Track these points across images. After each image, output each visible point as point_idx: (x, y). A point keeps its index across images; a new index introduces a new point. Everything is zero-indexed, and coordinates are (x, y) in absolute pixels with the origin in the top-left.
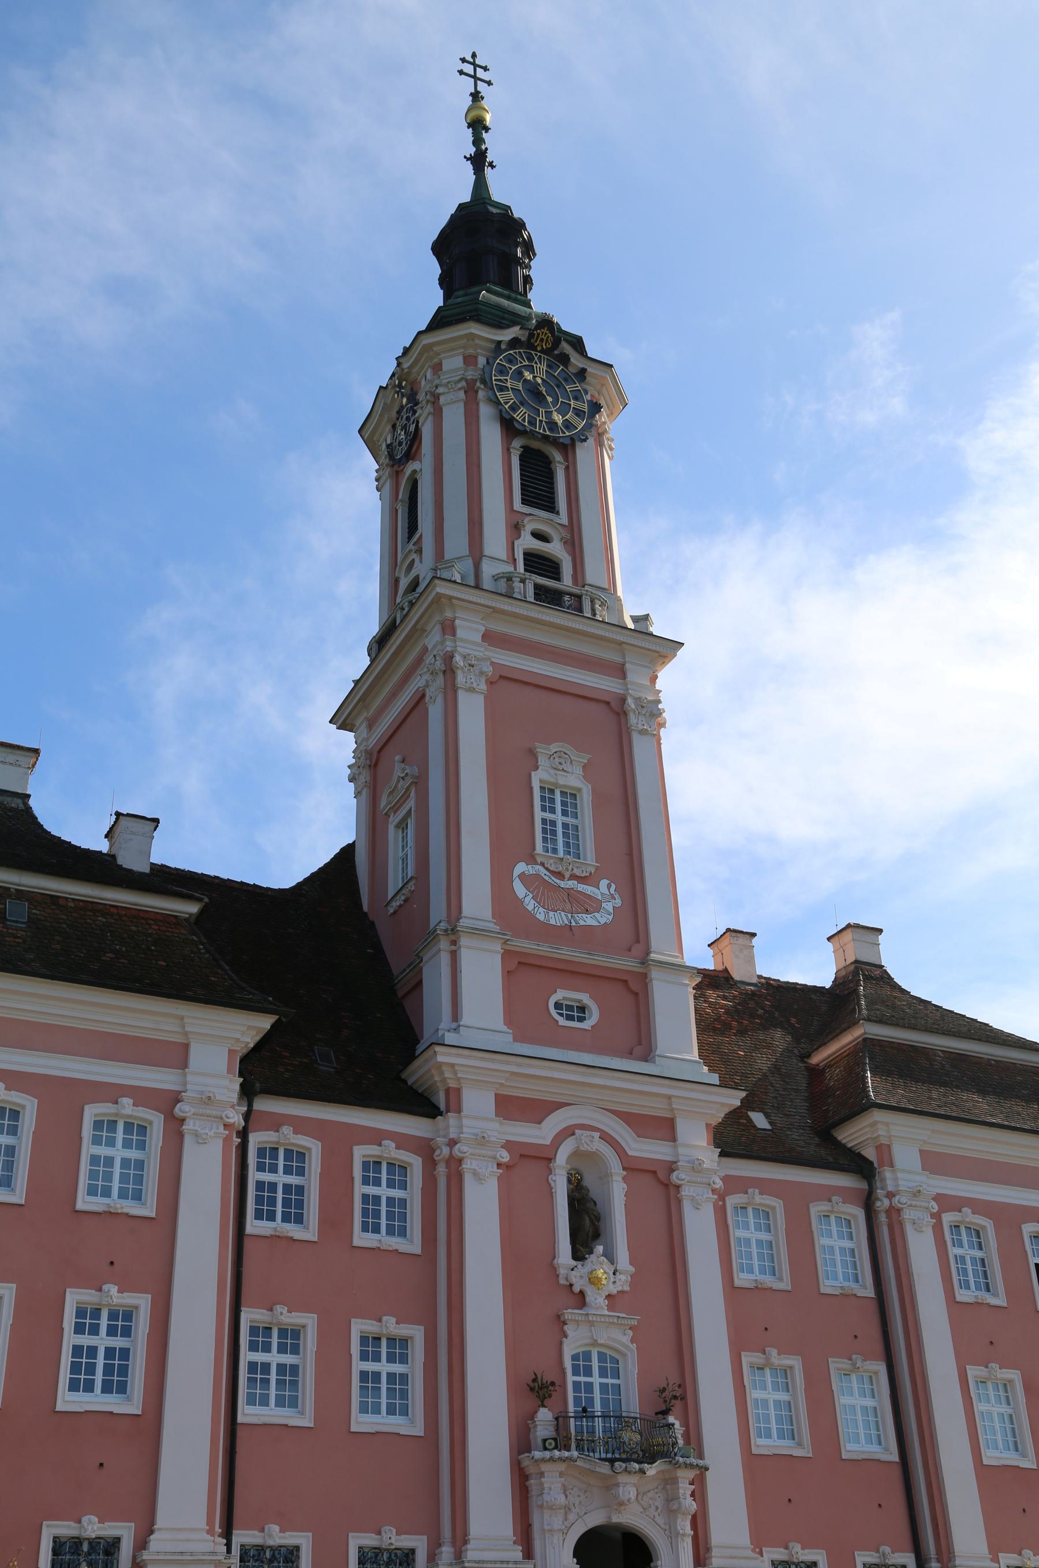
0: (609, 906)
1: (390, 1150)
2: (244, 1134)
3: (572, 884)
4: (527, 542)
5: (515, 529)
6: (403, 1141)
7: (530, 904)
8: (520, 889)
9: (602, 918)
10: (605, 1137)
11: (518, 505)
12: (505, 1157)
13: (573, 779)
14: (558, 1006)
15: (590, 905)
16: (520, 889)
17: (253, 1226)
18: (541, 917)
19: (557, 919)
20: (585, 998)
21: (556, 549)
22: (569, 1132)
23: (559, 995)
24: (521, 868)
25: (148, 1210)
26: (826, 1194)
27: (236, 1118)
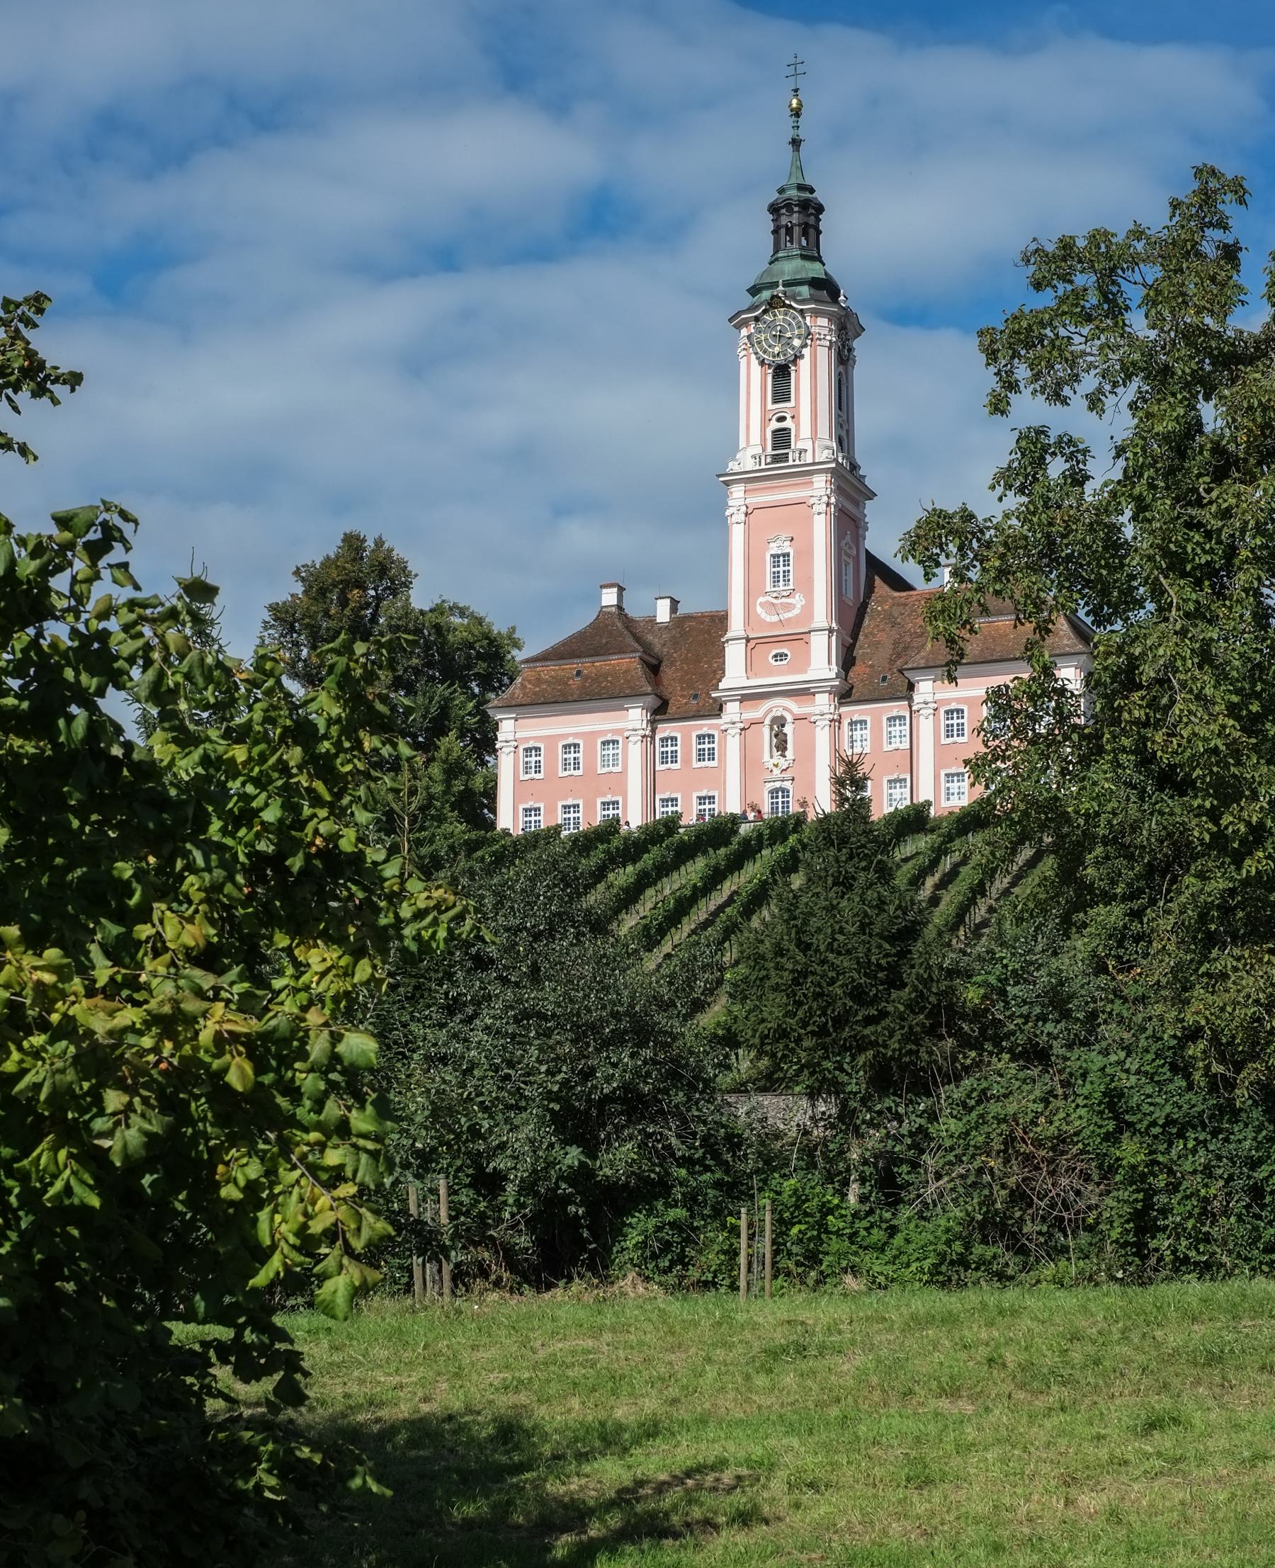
0: (799, 606)
1: (705, 731)
2: (653, 738)
3: (784, 600)
4: (775, 425)
5: (765, 422)
6: (711, 727)
7: (763, 615)
8: (759, 610)
9: (796, 611)
10: (785, 709)
11: (770, 406)
12: (742, 725)
13: (787, 548)
14: (776, 656)
15: (789, 607)
16: (759, 610)
17: (659, 767)
18: (768, 619)
19: (775, 619)
20: (786, 651)
21: (788, 423)
22: (770, 710)
23: (774, 652)
24: (761, 599)
25: (618, 769)
26: (892, 708)
27: (648, 733)
